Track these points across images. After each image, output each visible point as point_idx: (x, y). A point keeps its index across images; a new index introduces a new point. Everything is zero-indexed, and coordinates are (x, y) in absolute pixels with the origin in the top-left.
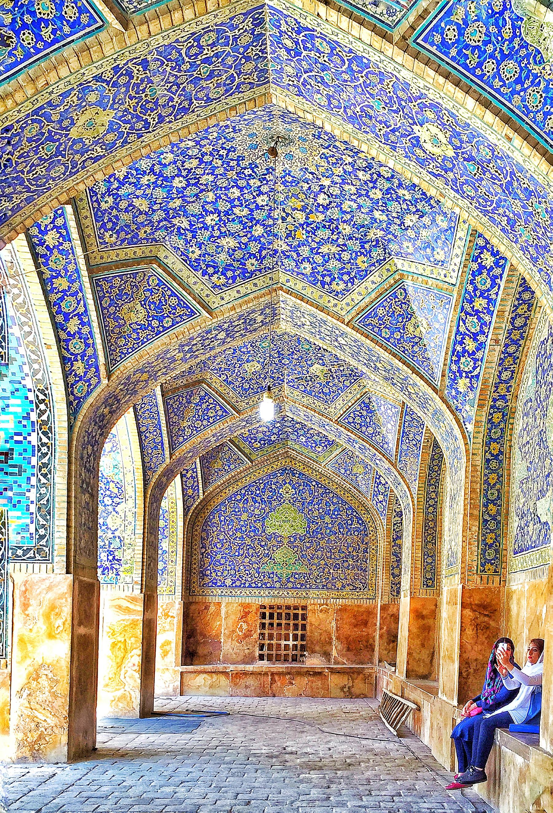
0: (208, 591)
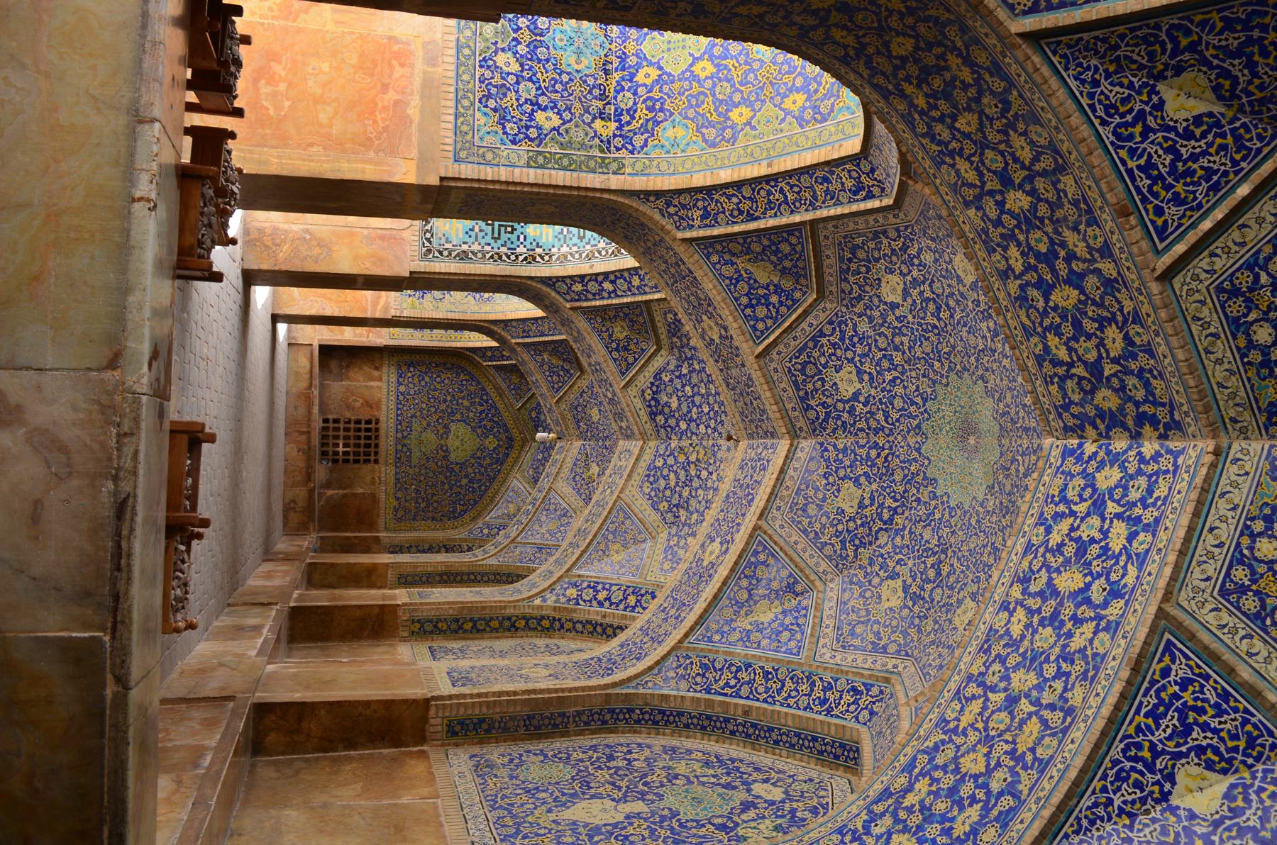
0: (393, 370)
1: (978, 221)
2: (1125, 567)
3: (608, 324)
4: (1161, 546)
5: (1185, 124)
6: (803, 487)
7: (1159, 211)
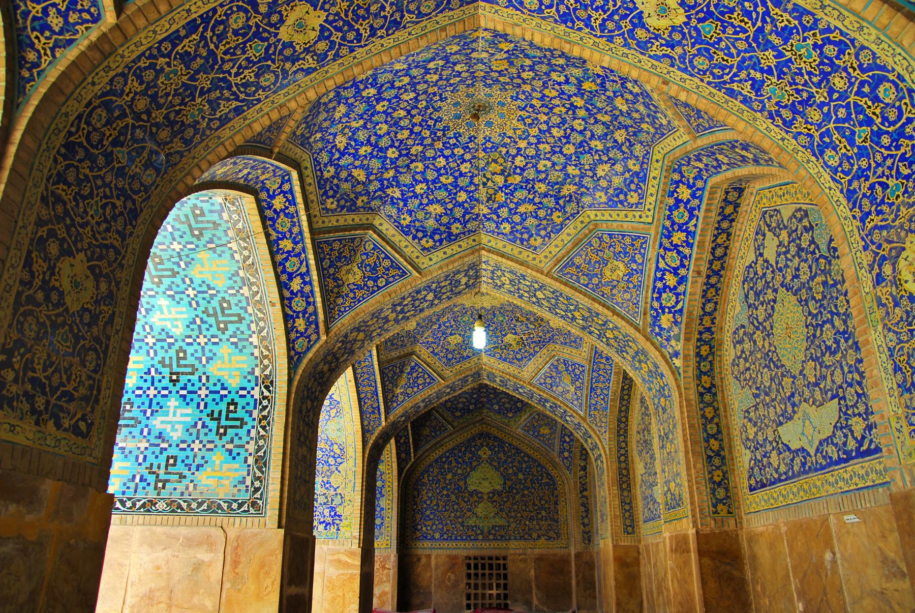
3: (345, 289)
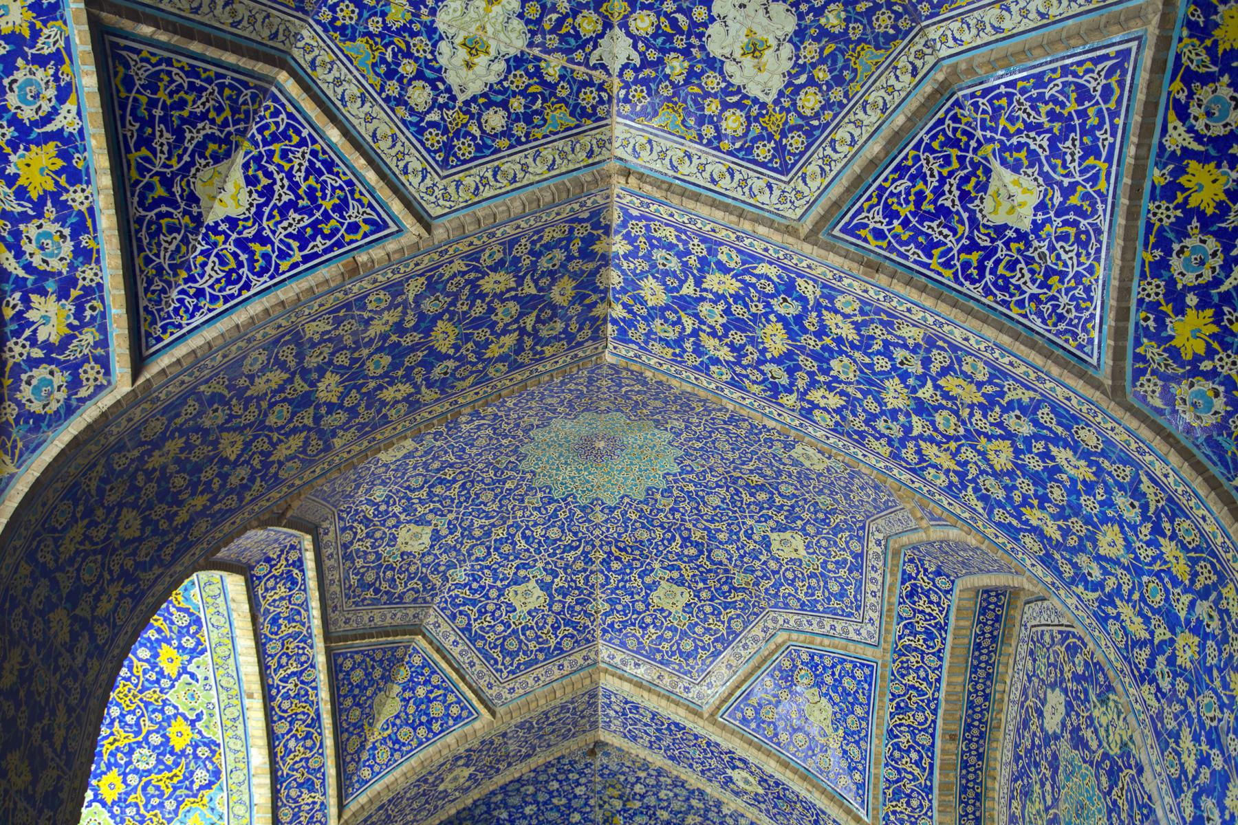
1: (349, 435)
2: (758, 277)
4: (733, 237)
5: (255, 195)
6: (658, 657)
7: (353, 228)
